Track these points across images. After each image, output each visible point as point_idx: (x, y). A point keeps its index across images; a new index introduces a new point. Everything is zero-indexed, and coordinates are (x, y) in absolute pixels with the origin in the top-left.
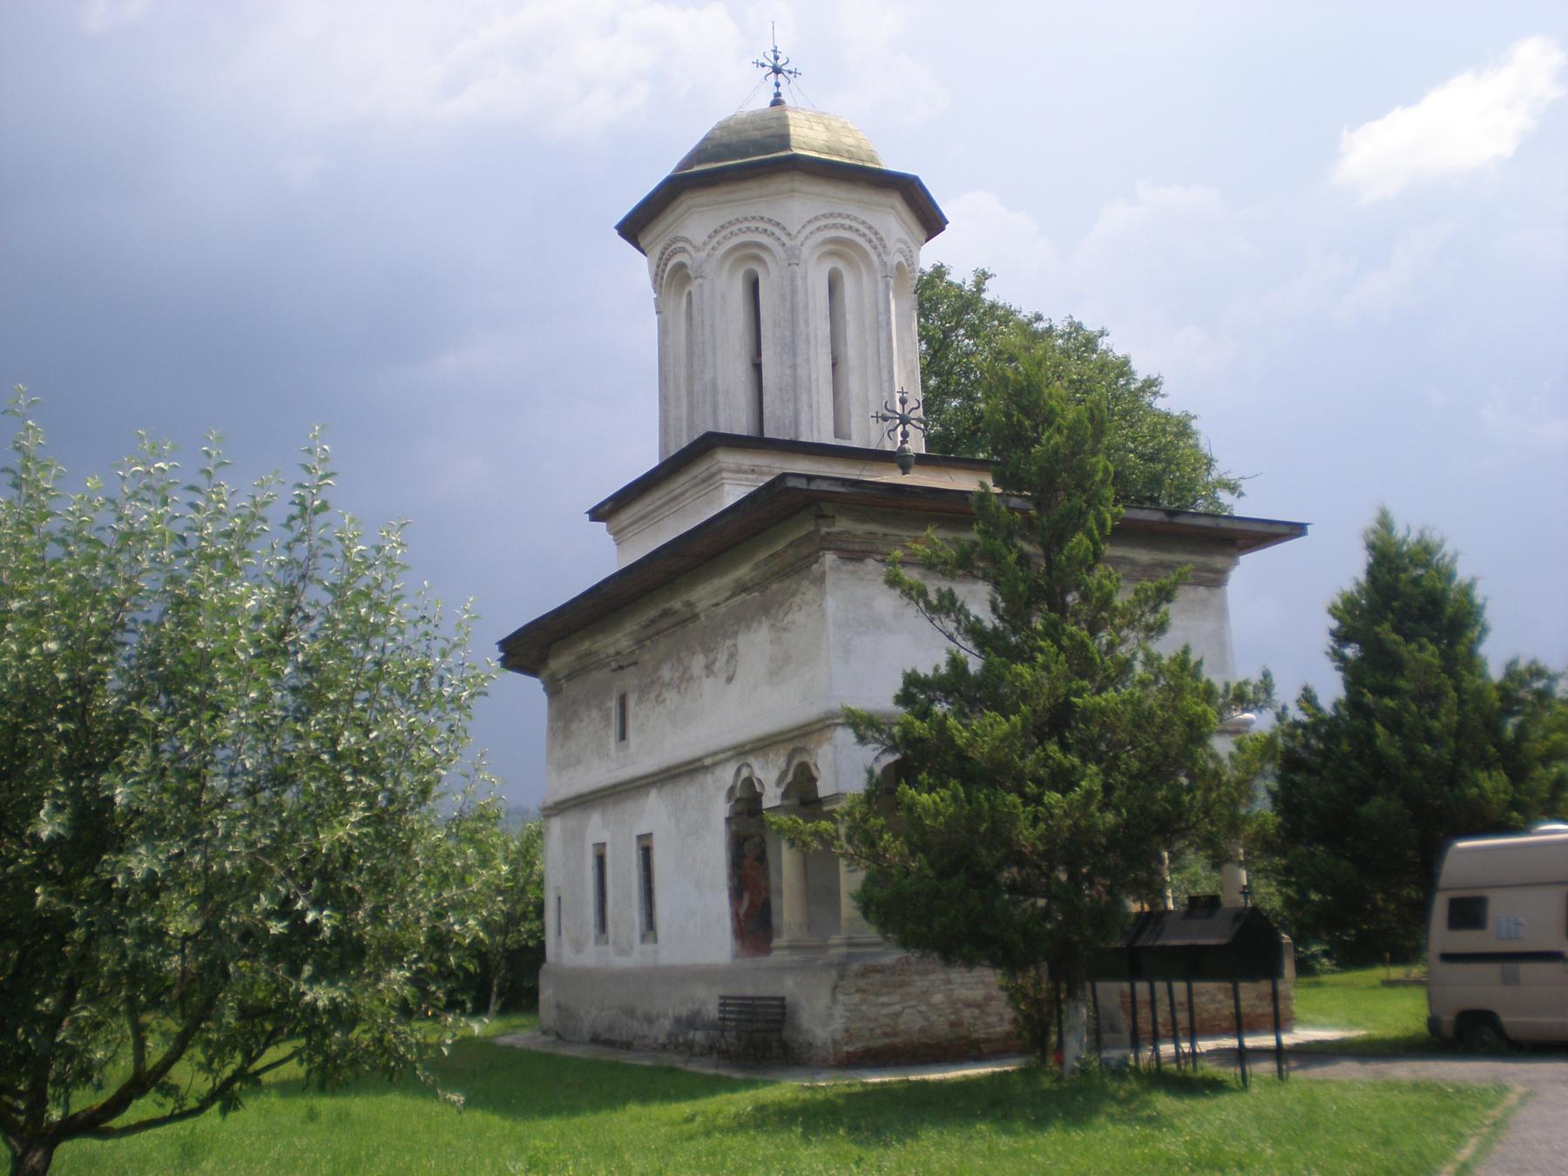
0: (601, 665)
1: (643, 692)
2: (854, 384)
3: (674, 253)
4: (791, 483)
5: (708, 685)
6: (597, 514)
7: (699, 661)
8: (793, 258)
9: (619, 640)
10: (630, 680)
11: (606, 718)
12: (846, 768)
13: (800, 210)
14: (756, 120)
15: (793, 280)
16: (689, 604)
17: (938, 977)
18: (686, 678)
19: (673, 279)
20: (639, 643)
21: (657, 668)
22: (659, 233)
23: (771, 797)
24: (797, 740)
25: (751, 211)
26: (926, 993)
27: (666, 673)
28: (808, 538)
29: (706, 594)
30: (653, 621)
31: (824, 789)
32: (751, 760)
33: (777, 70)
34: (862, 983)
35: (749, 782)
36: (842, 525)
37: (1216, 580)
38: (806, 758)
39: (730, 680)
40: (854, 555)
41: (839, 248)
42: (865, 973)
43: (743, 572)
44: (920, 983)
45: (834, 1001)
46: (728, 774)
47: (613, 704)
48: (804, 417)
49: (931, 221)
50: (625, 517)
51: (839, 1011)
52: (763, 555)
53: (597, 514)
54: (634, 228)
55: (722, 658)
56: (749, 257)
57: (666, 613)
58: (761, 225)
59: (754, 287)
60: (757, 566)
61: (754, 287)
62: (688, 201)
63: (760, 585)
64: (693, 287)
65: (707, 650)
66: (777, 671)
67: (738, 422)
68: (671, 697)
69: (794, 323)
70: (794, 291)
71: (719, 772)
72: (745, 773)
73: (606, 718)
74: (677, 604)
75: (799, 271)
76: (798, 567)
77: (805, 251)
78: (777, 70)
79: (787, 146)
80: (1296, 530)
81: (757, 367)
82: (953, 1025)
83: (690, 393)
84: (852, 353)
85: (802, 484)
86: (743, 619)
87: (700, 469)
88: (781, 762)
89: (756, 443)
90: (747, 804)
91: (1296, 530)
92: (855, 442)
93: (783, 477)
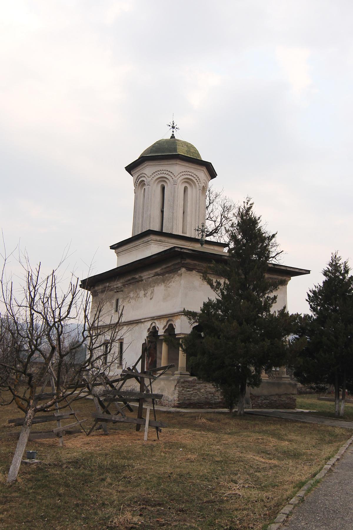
0: (112, 290)
1: (124, 299)
2: (188, 219)
3: (141, 177)
4: (176, 249)
5: (144, 299)
6: (112, 247)
7: (142, 293)
8: (175, 183)
9: (119, 284)
10: (120, 295)
11: (112, 305)
12: (183, 327)
13: (178, 170)
14: (167, 141)
15: (174, 189)
16: (141, 277)
17: (203, 385)
18: (138, 297)
19: (140, 184)
20: (124, 285)
21: (129, 293)
22: (138, 171)
23: (161, 332)
24: (170, 317)
25: (164, 168)
26: (199, 389)
27: (132, 295)
28: (178, 264)
29: (145, 275)
30: (129, 280)
31: (177, 331)
32: (156, 321)
33: (173, 127)
34: (183, 385)
35: (154, 328)
36: (188, 261)
37: (284, 283)
38: (172, 323)
39: (151, 299)
40: (190, 269)
41: (188, 181)
42: (183, 383)
43: (158, 270)
44: (198, 386)
45: (175, 389)
46: (148, 325)
47: (114, 301)
48: (175, 227)
49: (213, 174)
50: (120, 249)
51: (176, 392)
52: (164, 267)
53: (112, 247)
54: (130, 169)
55: (149, 293)
56: (163, 179)
57: (133, 278)
58: (167, 172)
59: (163, 188)
60: (162, 269)
61: (163, 188)
62: (146, 164)
63: (163, 274)
64: (146, 187)
65: (145, 290)
66: (165, 299)
67: (157, 228)
68: (133, 301)
69: (174, 201)
70: (175, 192)
71: (146, 323)
72: (154, 325)
73: (112, 305)
74: (137, 276)
75: (177, 186)
76: (174, 271)
77: (179, 181)
78: (173, 127)
79: (176, 151)
80: (308, 272)
81: (162, 212)
82: (206, 398)
83: (143, 217)
84: (189, 210)
85: (179, 250)
86: (156, 283)
87: (146, 239)
88: (165, 323)
89: (160, 233)
90: (153, 332)
91: (308, 272)
92: (188, 235)
93: (175, 247)
